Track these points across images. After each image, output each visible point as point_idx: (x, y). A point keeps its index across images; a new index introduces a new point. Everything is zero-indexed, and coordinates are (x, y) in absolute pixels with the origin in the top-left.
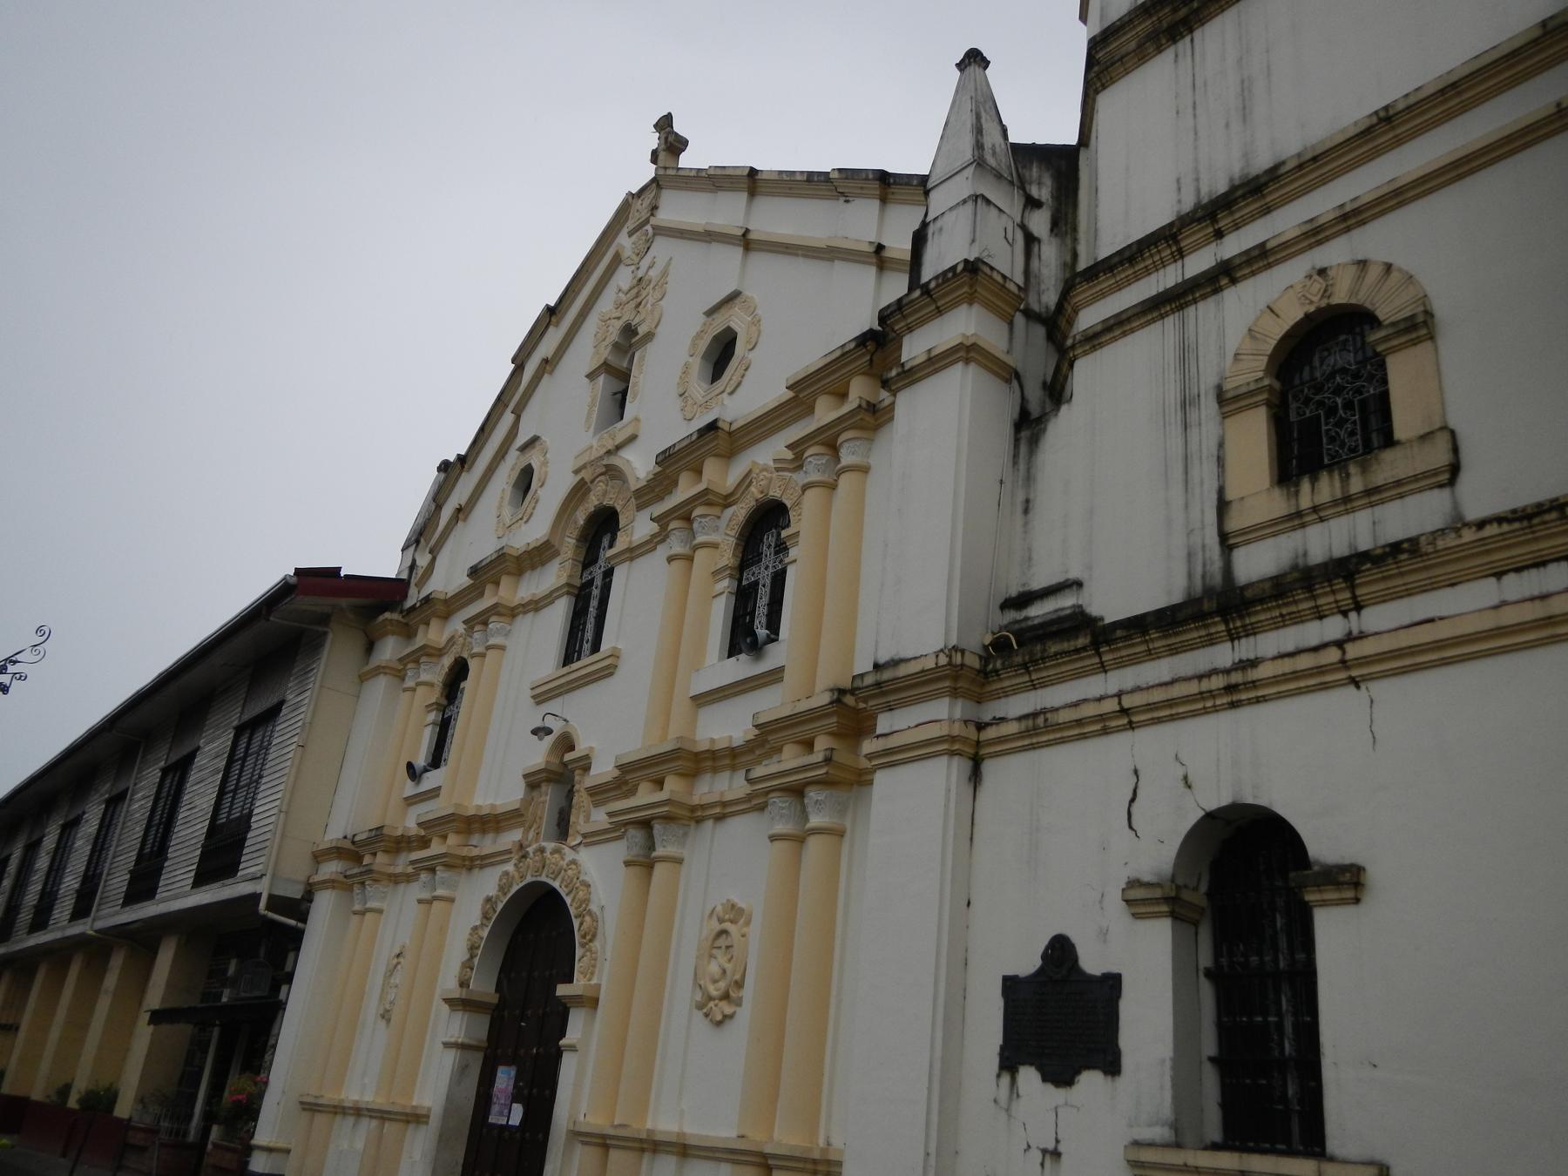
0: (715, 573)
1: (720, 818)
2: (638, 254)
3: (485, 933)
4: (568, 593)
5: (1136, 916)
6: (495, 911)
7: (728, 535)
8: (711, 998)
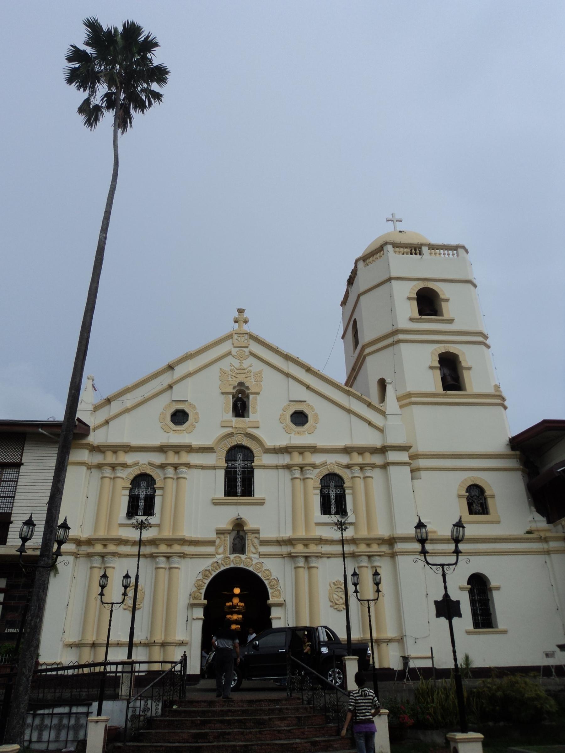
0: (314, 487)
1: (328, 558)
2: (241, 357)
3: (207, 582)
4: (224, 469)
5: (461, 590)
6: (211, 574)
7: (316, 477)
8: (336, 604)
